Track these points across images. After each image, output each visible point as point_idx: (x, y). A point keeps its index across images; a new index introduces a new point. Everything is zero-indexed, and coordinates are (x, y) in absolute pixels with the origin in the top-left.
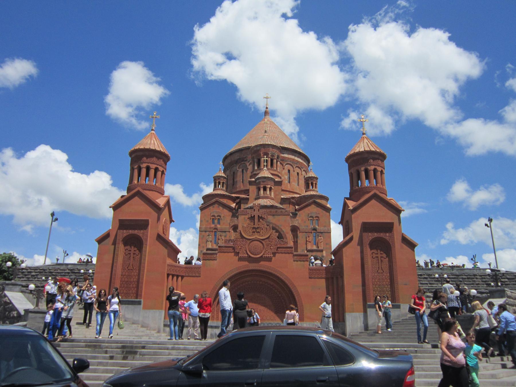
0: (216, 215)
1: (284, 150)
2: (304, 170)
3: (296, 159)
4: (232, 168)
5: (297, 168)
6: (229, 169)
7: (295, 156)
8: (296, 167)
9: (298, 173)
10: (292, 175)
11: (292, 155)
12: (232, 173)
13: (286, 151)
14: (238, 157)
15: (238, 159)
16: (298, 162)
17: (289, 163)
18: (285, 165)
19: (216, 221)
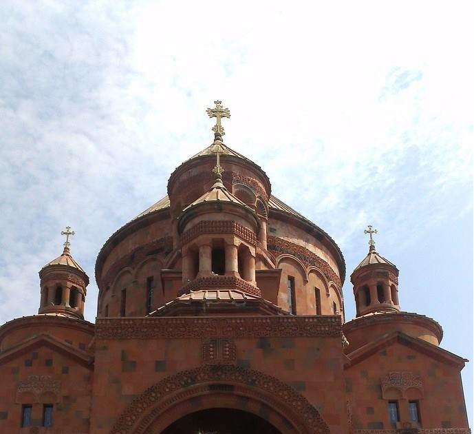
0: (37, 391)
1: (274, 220)
2: (332, 286)
3: (311, 248)
4: (118, 279)
5: (312, 275)
6: (110, 285)
7: (307, 241)
8: (311, 272)
9: (317, 291)
10: (300, 292)
11: (300, 237)
12: (119, 294)
13: (279, 222)
14: (137, 246)
15: (137, 250)
16: (315, 260)
17: (291, 256)
18: (279, 263)
19: (36, 414)
